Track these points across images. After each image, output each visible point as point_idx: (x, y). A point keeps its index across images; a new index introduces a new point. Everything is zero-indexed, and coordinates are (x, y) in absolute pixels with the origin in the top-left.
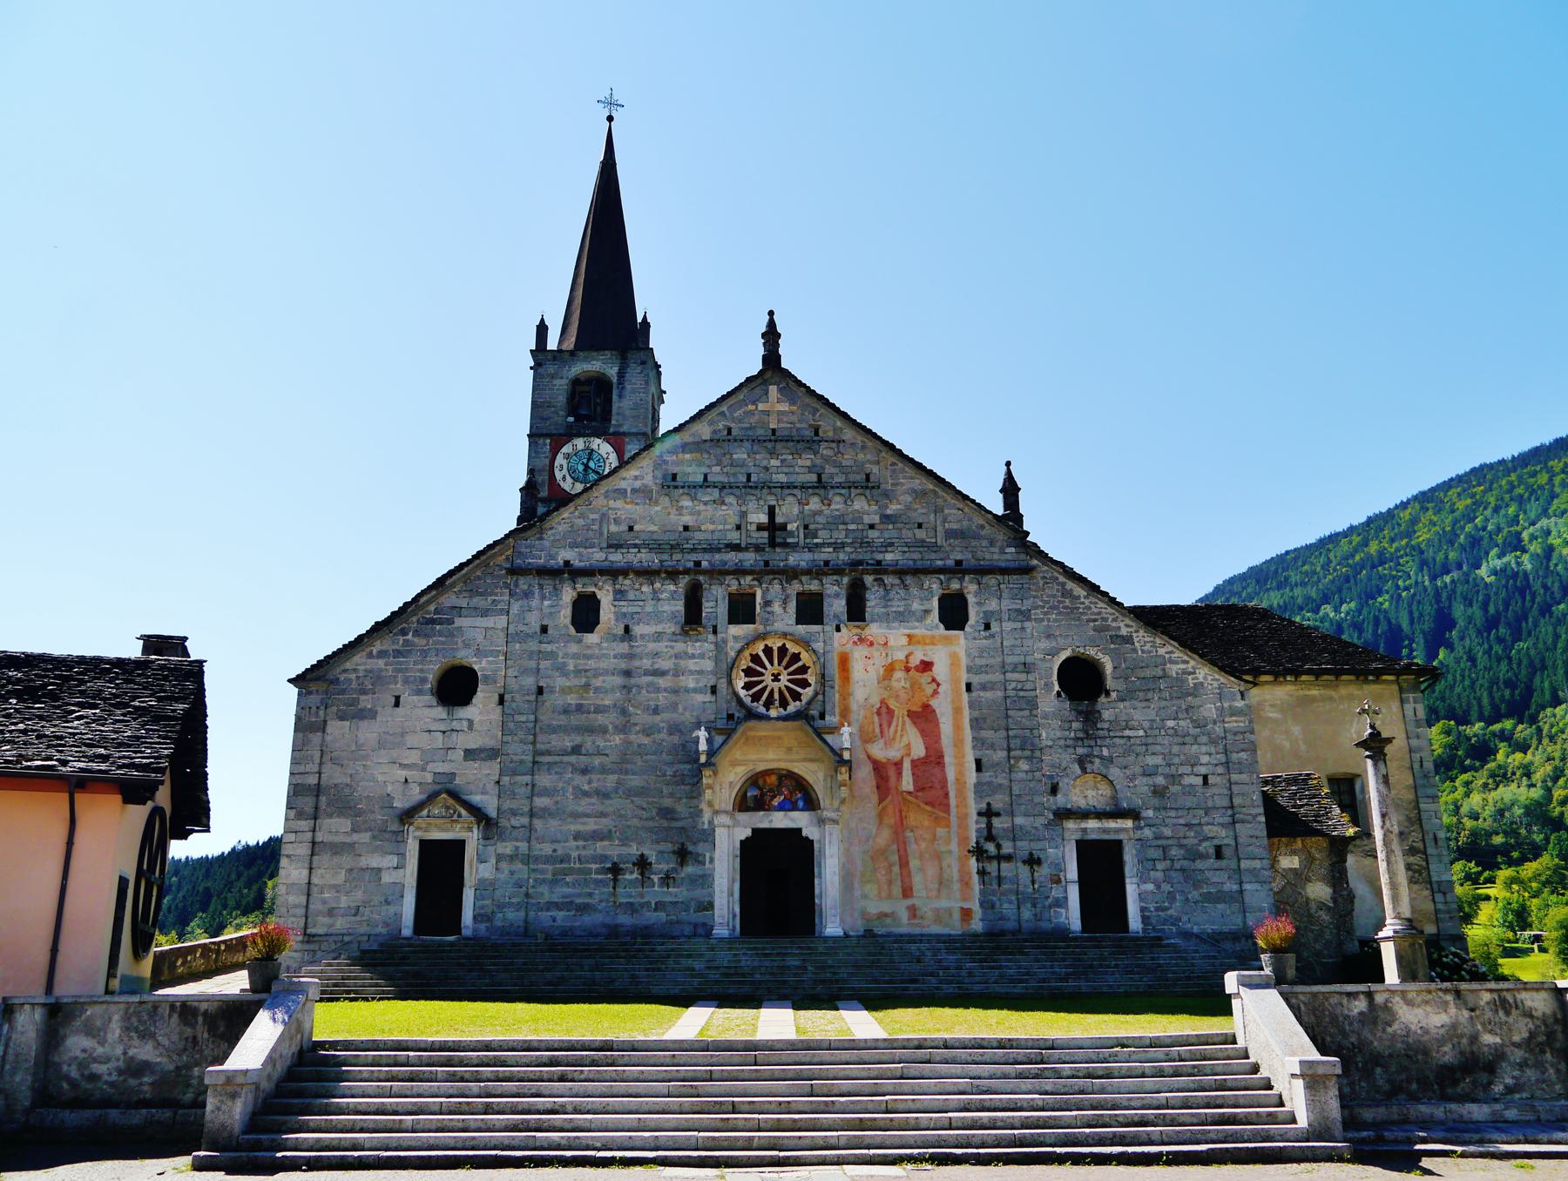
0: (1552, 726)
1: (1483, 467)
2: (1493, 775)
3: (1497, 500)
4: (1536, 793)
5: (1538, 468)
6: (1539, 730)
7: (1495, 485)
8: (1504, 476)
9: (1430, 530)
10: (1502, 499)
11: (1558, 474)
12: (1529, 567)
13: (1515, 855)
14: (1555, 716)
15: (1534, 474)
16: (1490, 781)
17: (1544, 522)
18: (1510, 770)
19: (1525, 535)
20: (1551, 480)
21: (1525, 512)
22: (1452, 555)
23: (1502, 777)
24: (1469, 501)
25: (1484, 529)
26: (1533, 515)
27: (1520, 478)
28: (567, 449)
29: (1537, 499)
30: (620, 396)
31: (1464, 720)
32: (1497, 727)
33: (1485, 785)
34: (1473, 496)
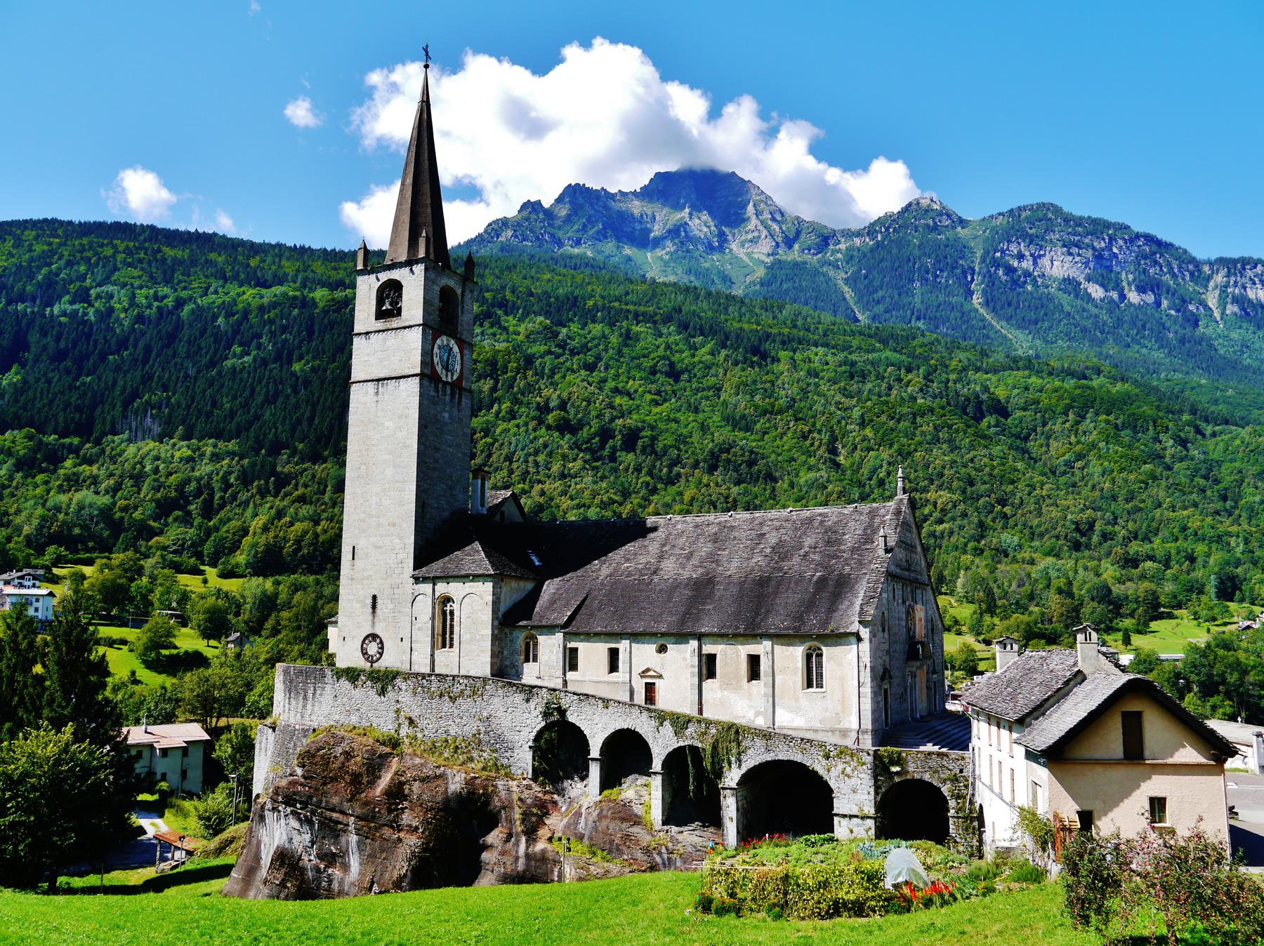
0: (112, 449)
1: (54, 221)
2: (68, 479)
3: (70, 255)
4: (105, 500)
5: (106, 242)
6: (103, 451)
7: (69, 243)
8: (77, 238)
9: (7, 260)
10: (74, 256)
11: (120, 252)
12: (93, 318)
13: (91, 544)
14: (114, 442)
15: (102, 246)
16: (65, 483)
17: (110, 288)
18: (82, 478)
19: (92, 292)
20: (114, 256)
21: (93, 273)
22: (29, 288)
23: (74, 482)
24: (45, 248)
25: (57, 275)
26: (99, 278)
27: (90, 243)
28: (439, 342)
29: (103, 267)
30: (462, 312)
31: (41, 430)
32: (67, 440)
33: (61, 486)
34: (50, 244)
